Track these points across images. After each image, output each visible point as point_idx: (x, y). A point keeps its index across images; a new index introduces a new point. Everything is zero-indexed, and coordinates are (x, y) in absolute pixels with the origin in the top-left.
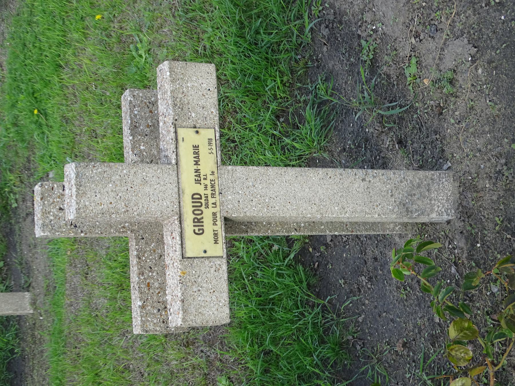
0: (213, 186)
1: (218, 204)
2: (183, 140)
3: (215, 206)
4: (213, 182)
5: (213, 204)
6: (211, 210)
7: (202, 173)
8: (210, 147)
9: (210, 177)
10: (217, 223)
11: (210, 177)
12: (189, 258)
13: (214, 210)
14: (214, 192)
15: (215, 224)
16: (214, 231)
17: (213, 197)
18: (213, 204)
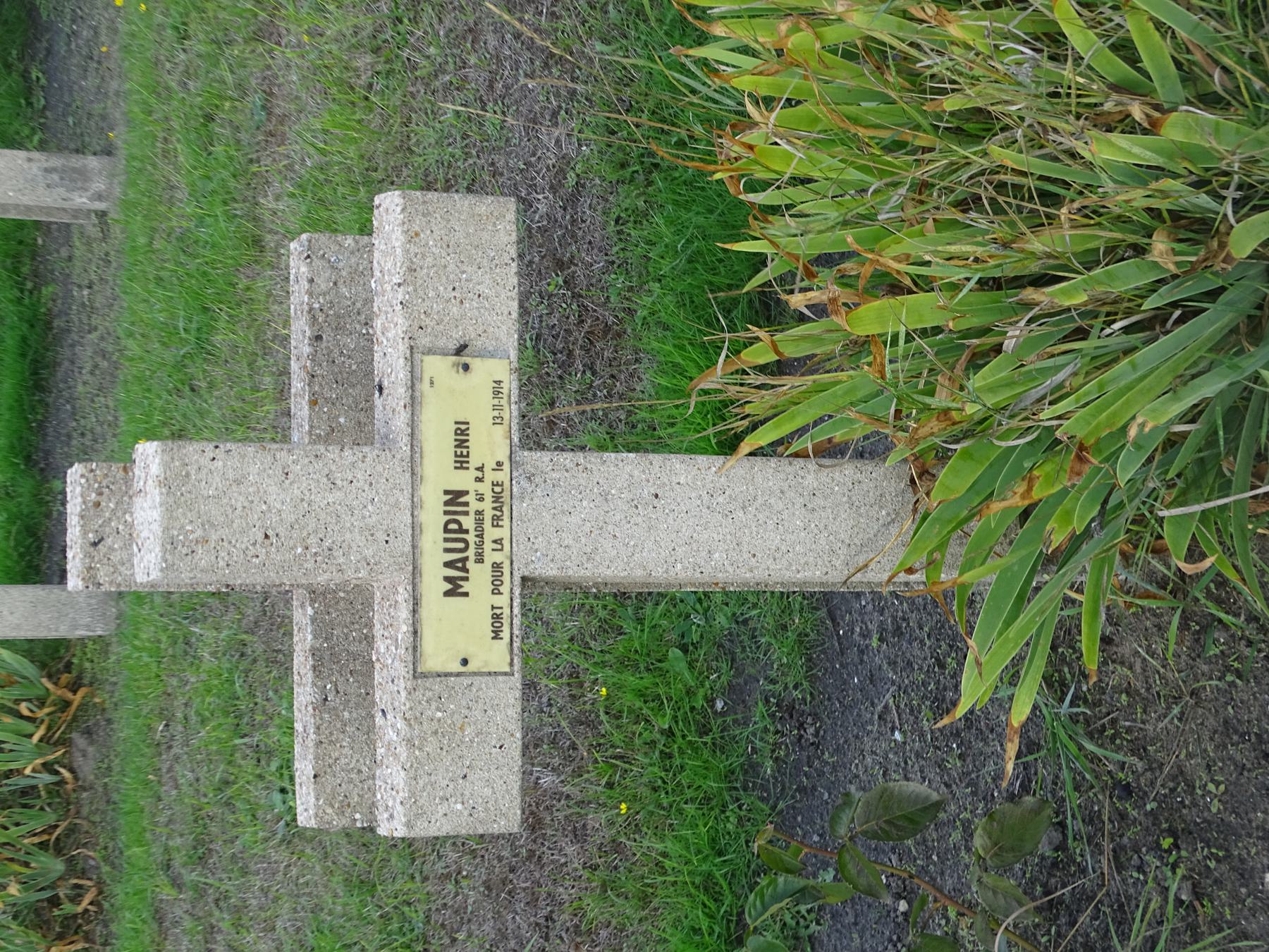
0: (497, 498)
2: (432, 383)
4: (498, 489)
5: (495, 542)
6: (491, 557)
7: (474, 461)
8: (496, 402)
9: (490, 476)
12: (425, 676)
13: (498, 557)
14: (499, 513)
15: (496, 591)
16: (493, 608)
17: (498, 526)
18: (495, 542)
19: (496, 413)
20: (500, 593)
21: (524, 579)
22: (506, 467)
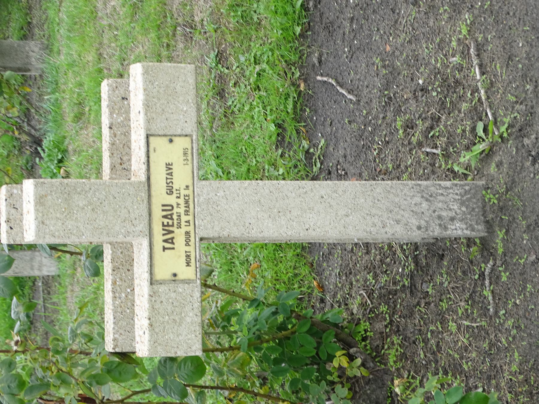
0: (187, 202)
1: (192, 223)
2: (155, 151)
3: (188, 224)
4: (187, 198)
5: (186, 222)
6: (184, 229)
7: (175, 186)
8: (185, 158)
9: (183, 192)
10: (190, 243)
11: (183, 192)
13: (188, 229)
14: (187, 209)
15: (187, 244)
17: (187, 215)
18: (186, 222)
19: (185, 162)
20: (189, 245)
21: (201, 239)
22: (191, 188)
